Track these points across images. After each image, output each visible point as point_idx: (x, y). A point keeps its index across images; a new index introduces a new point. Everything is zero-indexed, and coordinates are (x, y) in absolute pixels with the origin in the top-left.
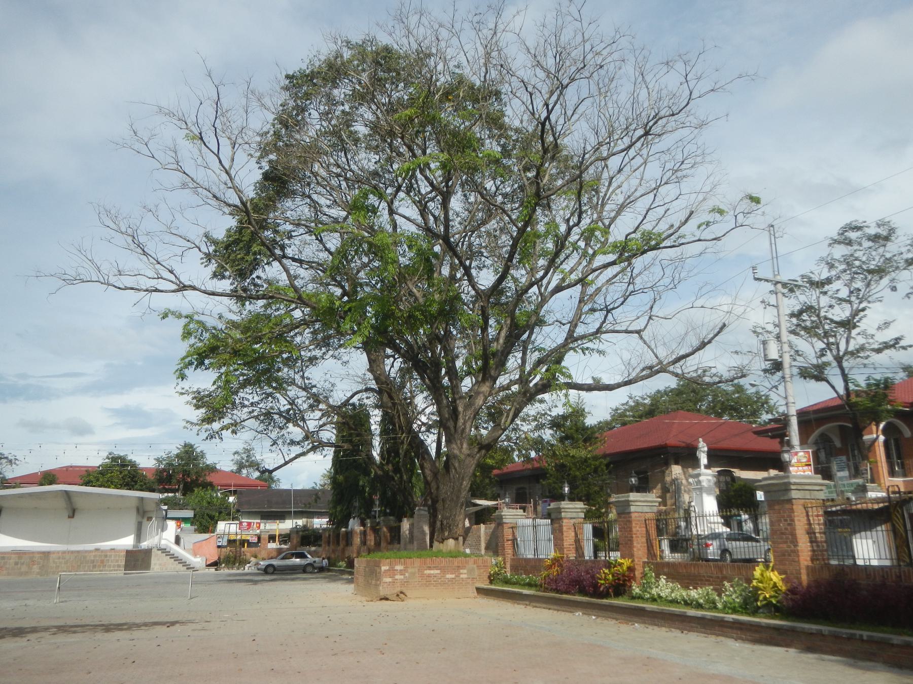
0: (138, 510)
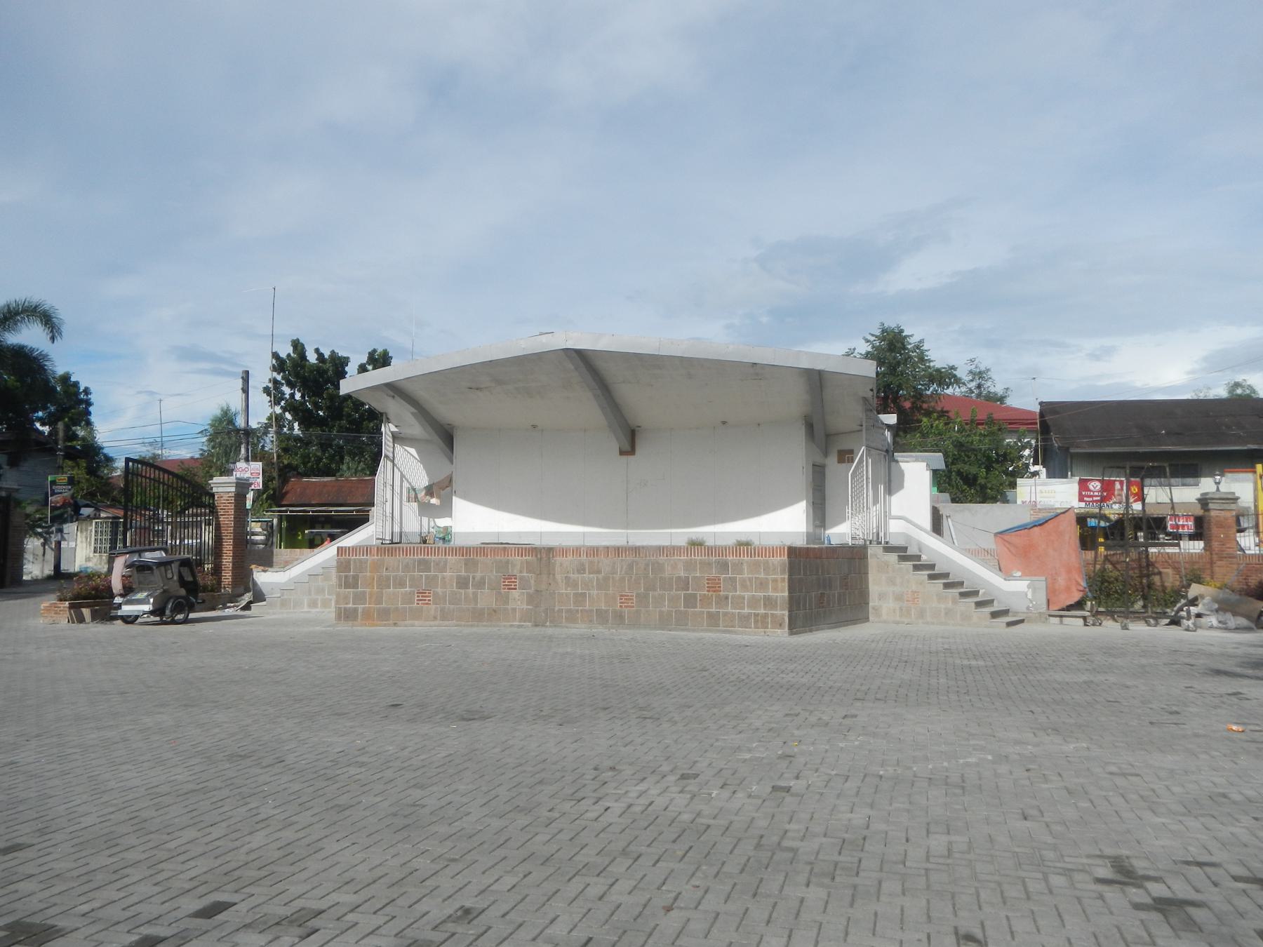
0: (810, 427)
